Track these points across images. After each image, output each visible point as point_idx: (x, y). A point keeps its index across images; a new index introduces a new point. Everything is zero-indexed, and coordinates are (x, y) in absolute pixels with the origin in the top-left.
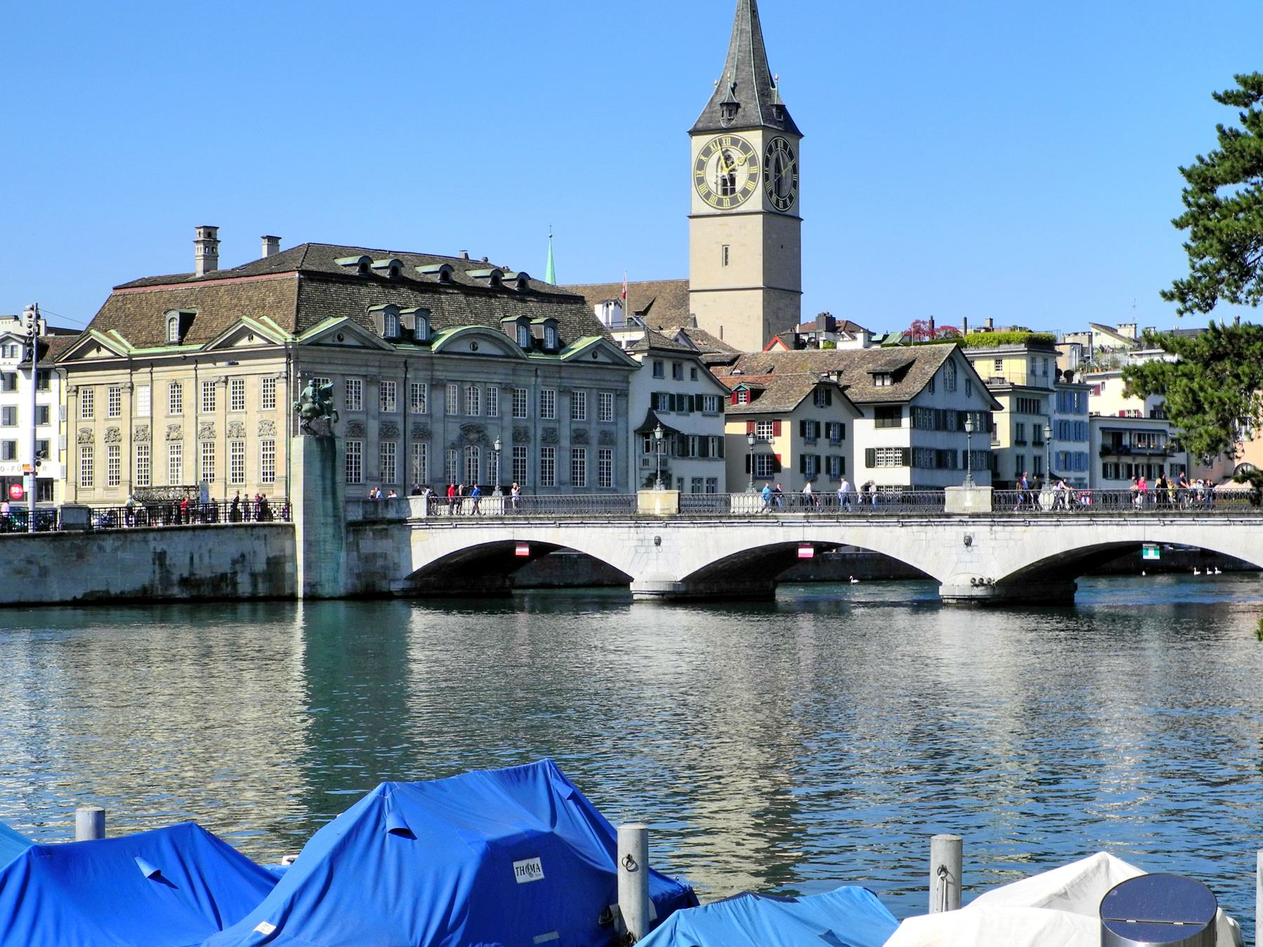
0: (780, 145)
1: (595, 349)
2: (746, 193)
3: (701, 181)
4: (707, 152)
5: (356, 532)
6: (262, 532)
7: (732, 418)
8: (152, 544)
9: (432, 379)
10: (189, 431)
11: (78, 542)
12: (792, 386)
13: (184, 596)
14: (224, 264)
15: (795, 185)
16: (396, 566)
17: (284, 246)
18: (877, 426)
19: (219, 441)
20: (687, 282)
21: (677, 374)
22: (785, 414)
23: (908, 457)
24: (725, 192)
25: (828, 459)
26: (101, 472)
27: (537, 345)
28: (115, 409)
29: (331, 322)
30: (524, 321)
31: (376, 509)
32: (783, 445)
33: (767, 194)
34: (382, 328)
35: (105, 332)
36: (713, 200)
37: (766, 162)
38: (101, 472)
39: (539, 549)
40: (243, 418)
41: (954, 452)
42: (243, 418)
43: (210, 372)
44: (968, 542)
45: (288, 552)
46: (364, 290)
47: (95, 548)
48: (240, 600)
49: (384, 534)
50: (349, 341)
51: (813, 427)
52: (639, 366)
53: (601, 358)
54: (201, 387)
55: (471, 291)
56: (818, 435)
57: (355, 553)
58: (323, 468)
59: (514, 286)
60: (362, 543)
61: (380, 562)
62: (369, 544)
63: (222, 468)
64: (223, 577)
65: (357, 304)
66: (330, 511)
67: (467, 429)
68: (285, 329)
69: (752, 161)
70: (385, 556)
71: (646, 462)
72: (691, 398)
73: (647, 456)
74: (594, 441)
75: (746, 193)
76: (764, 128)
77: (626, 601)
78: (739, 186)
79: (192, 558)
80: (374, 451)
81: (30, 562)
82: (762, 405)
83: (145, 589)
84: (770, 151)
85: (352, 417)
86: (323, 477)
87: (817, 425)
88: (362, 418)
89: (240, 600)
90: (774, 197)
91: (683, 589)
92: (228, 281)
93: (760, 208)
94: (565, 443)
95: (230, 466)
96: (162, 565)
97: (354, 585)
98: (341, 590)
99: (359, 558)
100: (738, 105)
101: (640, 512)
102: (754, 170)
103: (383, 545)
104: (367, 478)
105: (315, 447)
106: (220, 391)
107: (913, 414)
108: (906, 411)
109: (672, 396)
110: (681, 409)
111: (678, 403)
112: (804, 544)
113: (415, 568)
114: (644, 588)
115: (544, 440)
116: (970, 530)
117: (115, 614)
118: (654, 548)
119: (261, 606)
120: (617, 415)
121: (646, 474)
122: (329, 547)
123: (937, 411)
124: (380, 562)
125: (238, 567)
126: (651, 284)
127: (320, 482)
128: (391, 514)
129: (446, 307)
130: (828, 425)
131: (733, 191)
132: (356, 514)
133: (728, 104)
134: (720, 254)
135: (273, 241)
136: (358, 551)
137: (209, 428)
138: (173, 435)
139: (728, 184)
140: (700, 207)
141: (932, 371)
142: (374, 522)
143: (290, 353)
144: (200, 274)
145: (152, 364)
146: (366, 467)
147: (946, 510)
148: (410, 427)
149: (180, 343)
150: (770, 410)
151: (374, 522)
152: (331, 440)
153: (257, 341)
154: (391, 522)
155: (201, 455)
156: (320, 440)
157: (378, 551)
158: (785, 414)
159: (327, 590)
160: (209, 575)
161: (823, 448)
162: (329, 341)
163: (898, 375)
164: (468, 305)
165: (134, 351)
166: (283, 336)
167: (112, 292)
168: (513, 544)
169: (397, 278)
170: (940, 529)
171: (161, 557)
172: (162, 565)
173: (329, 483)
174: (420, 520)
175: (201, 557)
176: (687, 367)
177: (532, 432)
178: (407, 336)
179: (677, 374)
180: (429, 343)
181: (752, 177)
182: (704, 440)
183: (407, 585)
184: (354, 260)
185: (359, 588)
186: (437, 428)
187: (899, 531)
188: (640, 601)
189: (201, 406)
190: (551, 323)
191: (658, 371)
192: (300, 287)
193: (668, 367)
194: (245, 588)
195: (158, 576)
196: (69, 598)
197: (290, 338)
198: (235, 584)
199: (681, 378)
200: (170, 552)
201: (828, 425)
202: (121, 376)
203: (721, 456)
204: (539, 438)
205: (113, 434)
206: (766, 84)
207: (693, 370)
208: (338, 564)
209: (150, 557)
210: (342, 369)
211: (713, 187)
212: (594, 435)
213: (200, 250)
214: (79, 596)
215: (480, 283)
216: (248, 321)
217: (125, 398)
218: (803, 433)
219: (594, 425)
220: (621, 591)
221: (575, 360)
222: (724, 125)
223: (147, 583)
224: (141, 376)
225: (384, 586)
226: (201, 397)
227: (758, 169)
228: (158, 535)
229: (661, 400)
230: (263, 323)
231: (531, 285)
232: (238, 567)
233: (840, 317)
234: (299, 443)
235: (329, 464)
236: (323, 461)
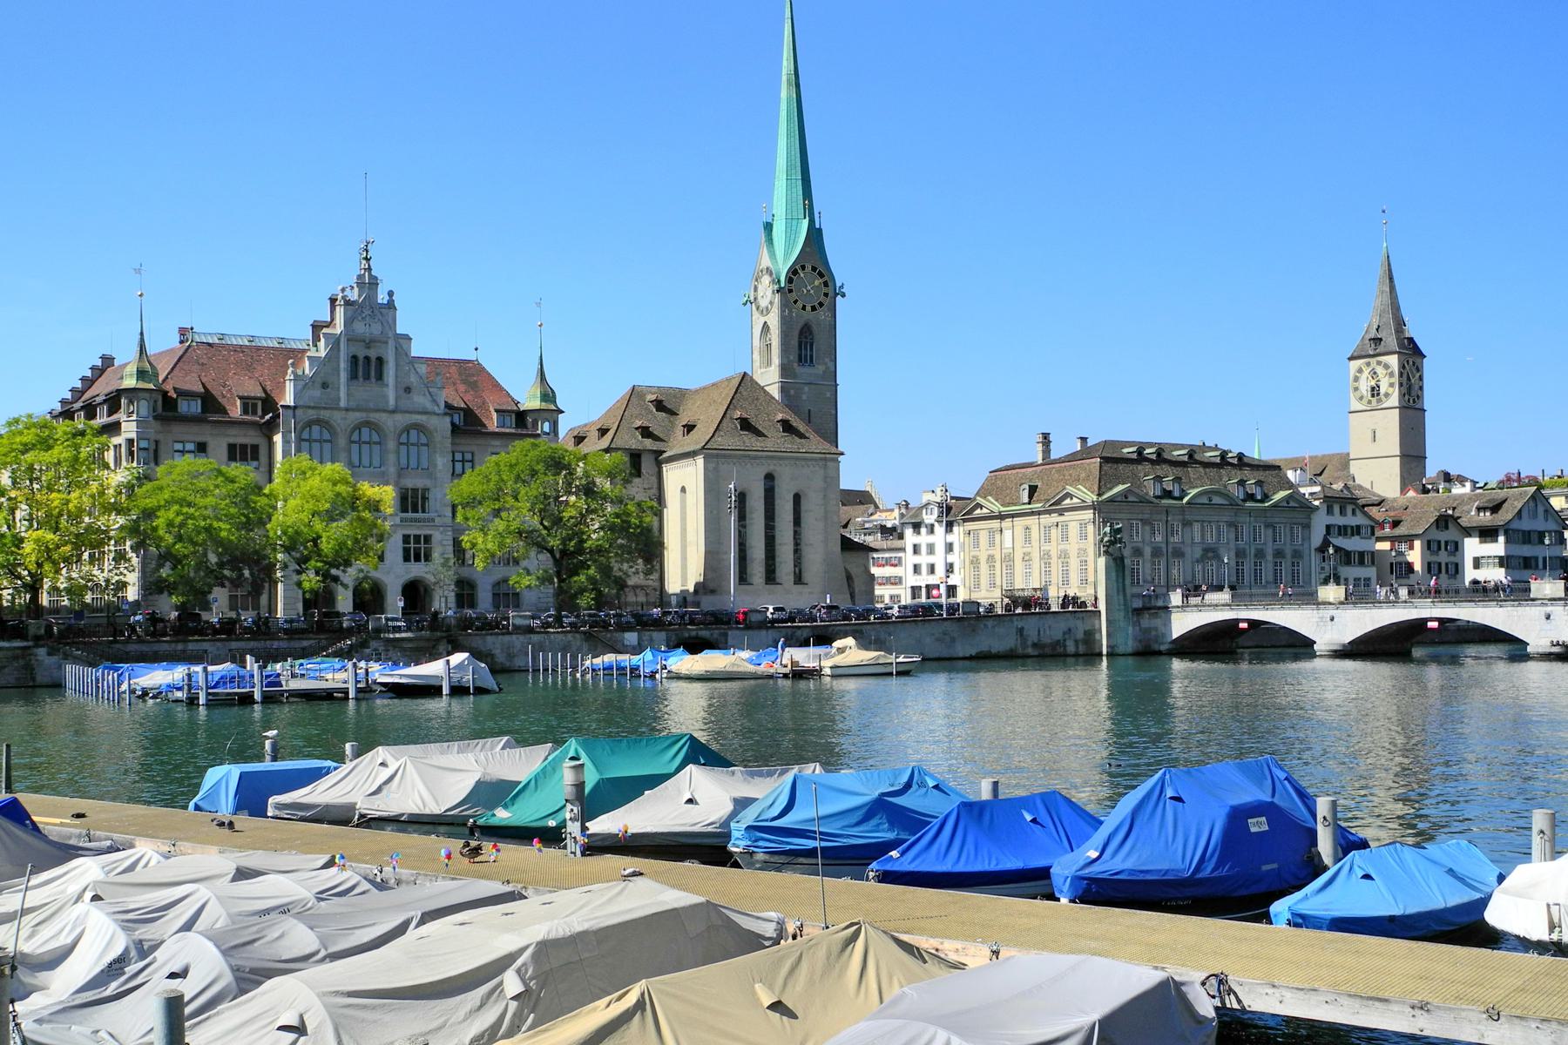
0: (1411, 363)
1: (1288, 499)
2: (1387, 395)
3: (1356, 389)
4: (1360, 371)
5: (1138, 615)
6: (1081, 615)
7: (1380, 539)
8: (1016, 623)
9: (1184, 520)
10: (1036, 555)
11: (972, 622)
12: (1421, 518)
13: (1036, 653)
14: (1054, 455)
15: (1421, 388)
16: (1164, 635)
17: (1090, 443)
18: (1481, 542)
19: (1054, 560)
20: (1348, 454)
21: (1342, 512)
22: (1417, 536)
23: (1503, 562)
24: (1373, 396)
25: (1447, 564)
26: (984, 581)
27: (1251, 497)
28: (992, 544)
29: (1121, 488)
30: (1242, 483)
32: (1415, 556)
33: (1402, 395)
34: (1151, 490)
35: (985, 498)
36: (1365, 401)
37: (1401, 375)
38: (984, 581)
39: (1254, 624)
40: (1068, 547)
41: (1536, 559)
42: (1068, 547)
43: (1047, 520)
44: (1548, 617)
45: (1097, 627)
46: (1140, 467)
47: (982, 626)
48: (1066, 655)
49: (1155, 616)
50: (1131, 498)
51: (1436, 544)
52: (1317, 508)
53: (1292, 504)
54: (1042, 529)
55: (1207, 465)
56: (1439, 549)
57: (1138, 628)
58: (1117, 576)
59: (1235, 461)
61: (1153, 633)
62: (1146, 621)
63: (1056, 577)
66: (1122, 602)
67: (1206, 550)
68: (1092, 492)
69: (1391, 374)
70: (1156, 629)
71: (1323, 568)
72: (1352, 527)
73: (1323, 564)
74: (1289, 556)
75: (1387, 395)
76: (1399, 353)
77: (1312, 655)
78: (1382, 391)
80: (1148, 565)
81: (945, 634)
82: (1401, 530)
83: (1011, 650)
84: (1404, 367)
85: (1134, 545)
86: (1117, 581)
87: (1439, 542)
88: (1140, 545)
89: (1066, 655)
90: (1407, 397)
91: (1349, 648)
92: (1057, 465)
93: (1397, 404)
94: (1270, 558)
95: (1060, 576)
96: (1021, 635)
98: (1130, 650)
99: (1140, 630)
100: (1381, 339)
101: (1320, 600)
102: (1392, 380)
103: (1157, 622)
104: (1144, 582)
105: (1112, 563)
106: (1054, 531)
107: (1506, 533)
108: (1501, 532)
109: (1339, 527)
110: (1346, 534)
111: (1343, 531)
112: (1432, 619)
113: (1175, 636)
114: (1323, 648)
115: (1256, 556)
116: (1549, 609)
117: (995, 663)
118: (1330, 622)
119: (1081, 659)
120: (1303, 539)
121: (1323, 576)
122: (1122, 624)
123: (1524, 532)
124: (1153, 633)
125: (1067, 636)
126: (1324, 456)
127: (1115, 584)
128: (1160, 603)
129: (1192, 476)
130: (1446, 543)
131: (1378, 394)
132: (1138, 604)
133: (1374, 339)
134: (1370, 435)
135: (1084, 440)
137: (1048, 554)
138: (1027, 558)
139: (1375, 391)
140: (1356, 405)
141: (1519, 506)
142: (1149, 609)
143: (1094, 507)
144: (1040, 462)
145: (1013, 516)
146: (1143, 576)
147: (1532, 596)
148: (1170, 550)
149: (1029, 503)
150: (1406, 533)
151: (1149, 609)
152: (1122, 559)
153: (1075, 500)
154: (1159, 608)
155: (1043, 569)
156: (1115, 559)
157: (1152, 626)
158: (1417, 536)
159: (1121, 650)
160: (1049, 641)
161: (1443, 557)
162: (1119, 499)
163: (1495, 509)
164: (1206, 474)
165: (1002, 509)
166: (1091, 497)
167: (988, 474)
168: (1238, 621)
169: (1161, 458)
170: (1527, 608)
171: (1021, 631)
172: (1021, 635)
173: (1121, 585)
174: (1178, 607)
176: (1349, 509)
178: (1167, 494)
179: (1342, 512)
180: (1181, 498)
181: (1392, 385)
182: (1362, 554)
183: (1171, 646)
184: (1134, 449)
185: (1140, 648)
186: (1188, 550)
187: (1498, 610)
188: (1321, 656)
189: (1043, 541)
190: (1259, 483)
191: (1330, 511)
192: (1101, 467)
193: (1336, 509)
194: (1071, 648)
196: (967, 655)
197: (1095, 498)
198: (1065, 646)
199: (1345, 515)
200: (1026, 627)
201: (1446, 543)
202: (995, 524)
203: (1373, 563)
205: (991, 558)
206: (1400, 324)
207: (1353, 510)
209: (1014, 630)
210: (1129, 516)
211: (1365, 393)
212: (1288, 552)
213: (1040, 447)
215: (1213, 460)
216: (1070, 489)
217: (997, 536)
218: (1429, 548)
219: (1288, 545)
220: (1309, 650)
221: (1275, 506)
222: (1371, 353)
223: (1013, 646)
224: (1007, 523)
225: (1156, 647)
226: (1042, 535)
227: (1396, 380)
228: (1019, 618)
229: (1332, 530)
230: (1079, 489)
231: (1245, 460)
233: (1453, 472)
234: (1102, 561)
236: (1117, 571)
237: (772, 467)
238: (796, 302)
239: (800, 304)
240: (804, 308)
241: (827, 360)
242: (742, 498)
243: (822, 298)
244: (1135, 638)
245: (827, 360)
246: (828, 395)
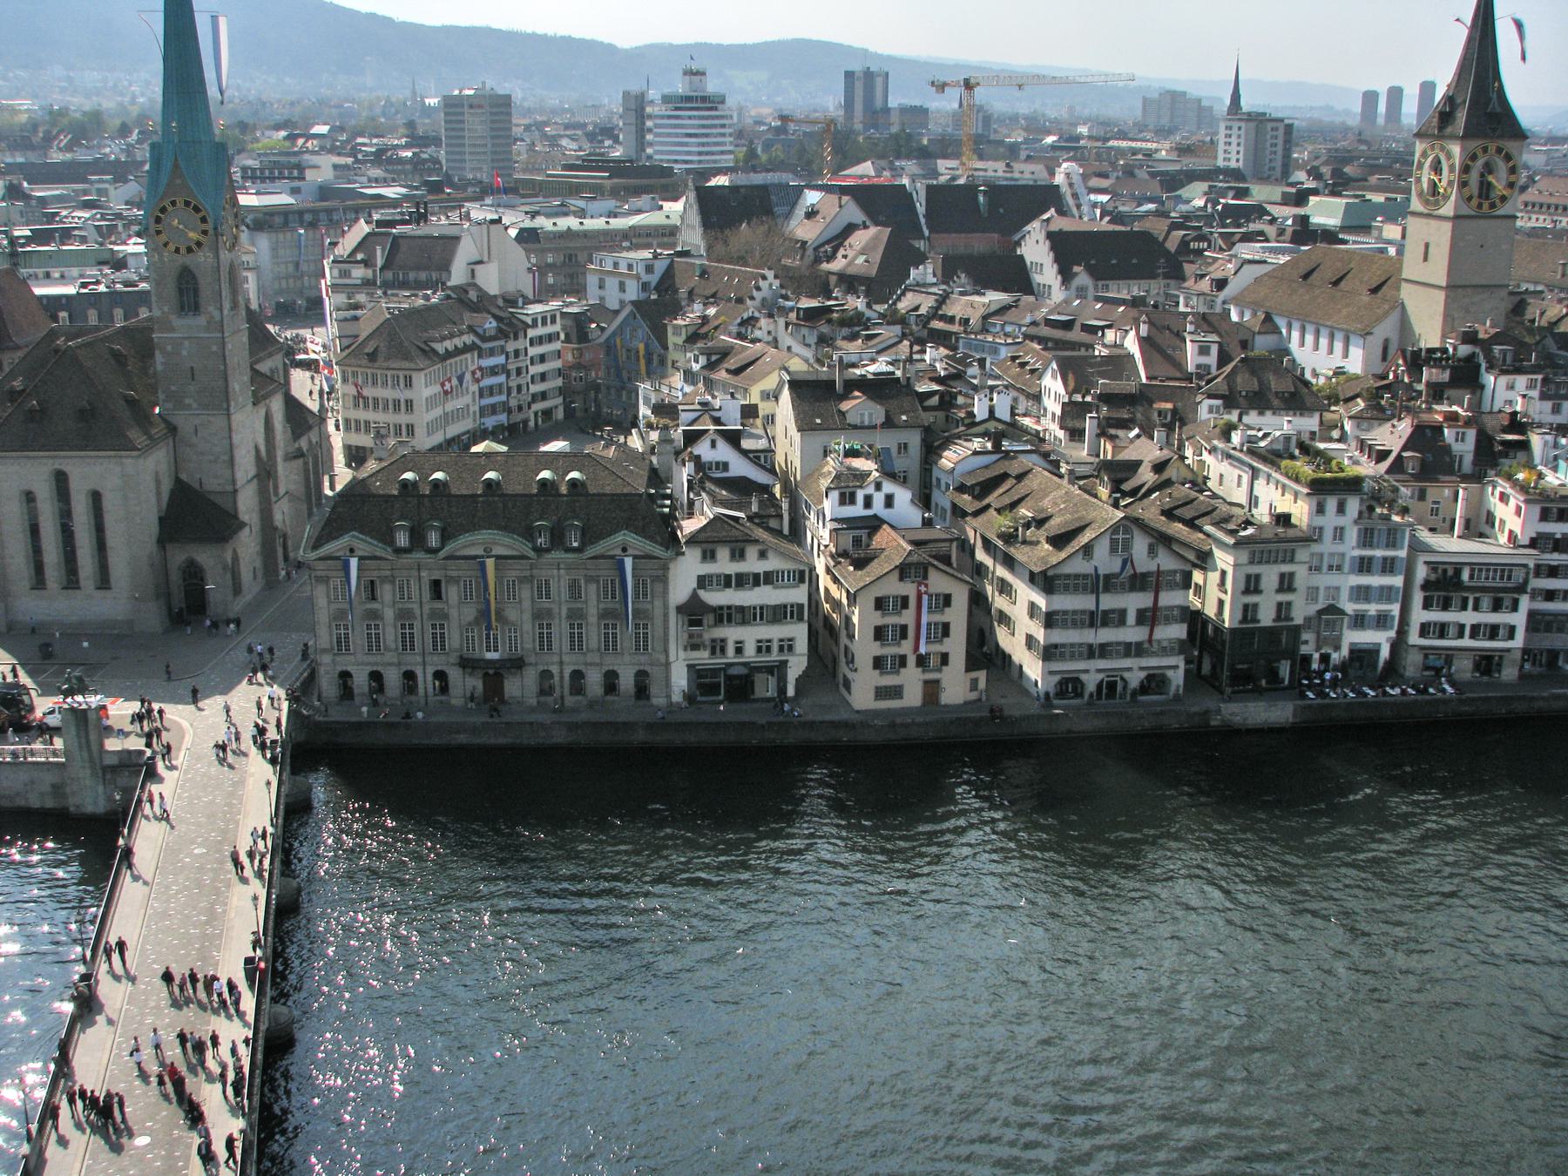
62: (123, 780)
86: (78, 736)
94: (593, 619)
115: (569, 617)
122: (88, 782)
186: (454, 613)
193: (723, 553)
236: (78, 725)
238: (166, 245)
239: (172, 247)
240: (177, 250)
241: (211, 309)
242: (30, 497)
243: (201, 238)
245: (211, 309)
246: (214, 348)
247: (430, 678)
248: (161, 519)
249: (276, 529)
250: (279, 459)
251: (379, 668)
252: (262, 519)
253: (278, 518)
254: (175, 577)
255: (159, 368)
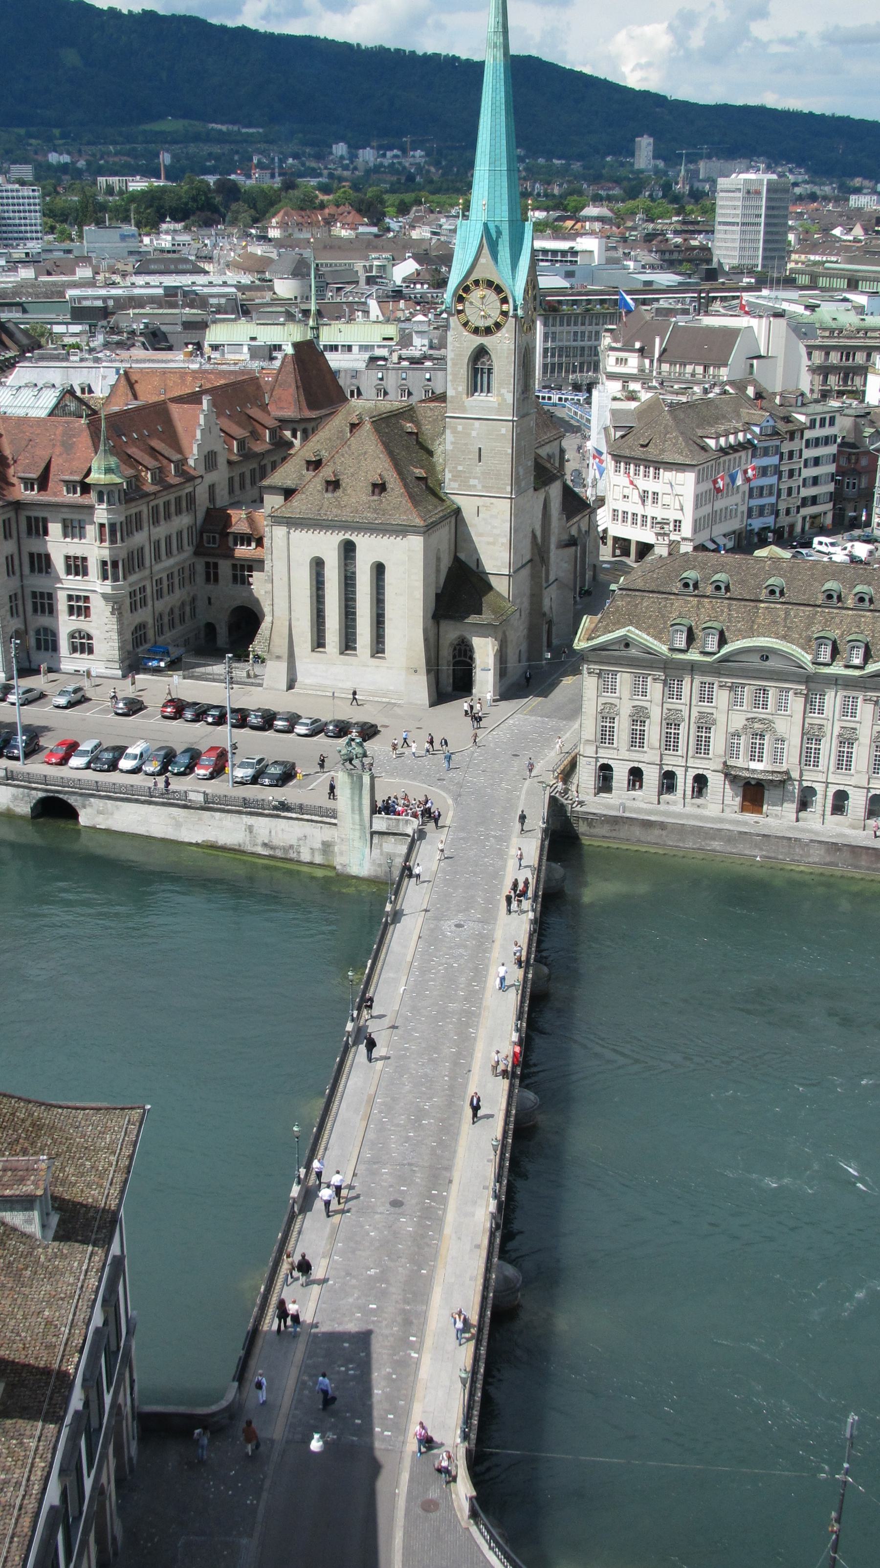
31: (398, 825)
57: (379, 851)
58: (353, 794)
60: (384, 844)
64: (291, 847)
65: (663, 616)
79: (270, 832)
86: (352, 800)
96: (251, 832)
97: (375, 871)
99: (381, 854)
125: (301, 842)
127: (350, 802)
136: (381, 849)
148: (694, 714)
171: (250, 829)
172: (251, 832)
173: (356, 804)
175: (276, 832)
177: (827, 729)
195: (248, 839)
196: (194, 841)
200: (255, 825)
204: (836, 733)
208: (363, 856)
214: (200, 842)
223: (241, 841)
232: (301, 842)
235: (357, 792)
236: (352, 789)
237: (347, 536)
242: (318, 565)
244: (373, 862)
247: (690, 781)
248: (437, 595)
249: (544, 614)
250: (553, 546)
251: (640, 765)
252: (532, 603)
253: (546, 602)
254: (446, 653)
255: (449, 447)
